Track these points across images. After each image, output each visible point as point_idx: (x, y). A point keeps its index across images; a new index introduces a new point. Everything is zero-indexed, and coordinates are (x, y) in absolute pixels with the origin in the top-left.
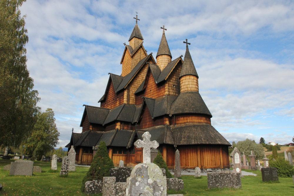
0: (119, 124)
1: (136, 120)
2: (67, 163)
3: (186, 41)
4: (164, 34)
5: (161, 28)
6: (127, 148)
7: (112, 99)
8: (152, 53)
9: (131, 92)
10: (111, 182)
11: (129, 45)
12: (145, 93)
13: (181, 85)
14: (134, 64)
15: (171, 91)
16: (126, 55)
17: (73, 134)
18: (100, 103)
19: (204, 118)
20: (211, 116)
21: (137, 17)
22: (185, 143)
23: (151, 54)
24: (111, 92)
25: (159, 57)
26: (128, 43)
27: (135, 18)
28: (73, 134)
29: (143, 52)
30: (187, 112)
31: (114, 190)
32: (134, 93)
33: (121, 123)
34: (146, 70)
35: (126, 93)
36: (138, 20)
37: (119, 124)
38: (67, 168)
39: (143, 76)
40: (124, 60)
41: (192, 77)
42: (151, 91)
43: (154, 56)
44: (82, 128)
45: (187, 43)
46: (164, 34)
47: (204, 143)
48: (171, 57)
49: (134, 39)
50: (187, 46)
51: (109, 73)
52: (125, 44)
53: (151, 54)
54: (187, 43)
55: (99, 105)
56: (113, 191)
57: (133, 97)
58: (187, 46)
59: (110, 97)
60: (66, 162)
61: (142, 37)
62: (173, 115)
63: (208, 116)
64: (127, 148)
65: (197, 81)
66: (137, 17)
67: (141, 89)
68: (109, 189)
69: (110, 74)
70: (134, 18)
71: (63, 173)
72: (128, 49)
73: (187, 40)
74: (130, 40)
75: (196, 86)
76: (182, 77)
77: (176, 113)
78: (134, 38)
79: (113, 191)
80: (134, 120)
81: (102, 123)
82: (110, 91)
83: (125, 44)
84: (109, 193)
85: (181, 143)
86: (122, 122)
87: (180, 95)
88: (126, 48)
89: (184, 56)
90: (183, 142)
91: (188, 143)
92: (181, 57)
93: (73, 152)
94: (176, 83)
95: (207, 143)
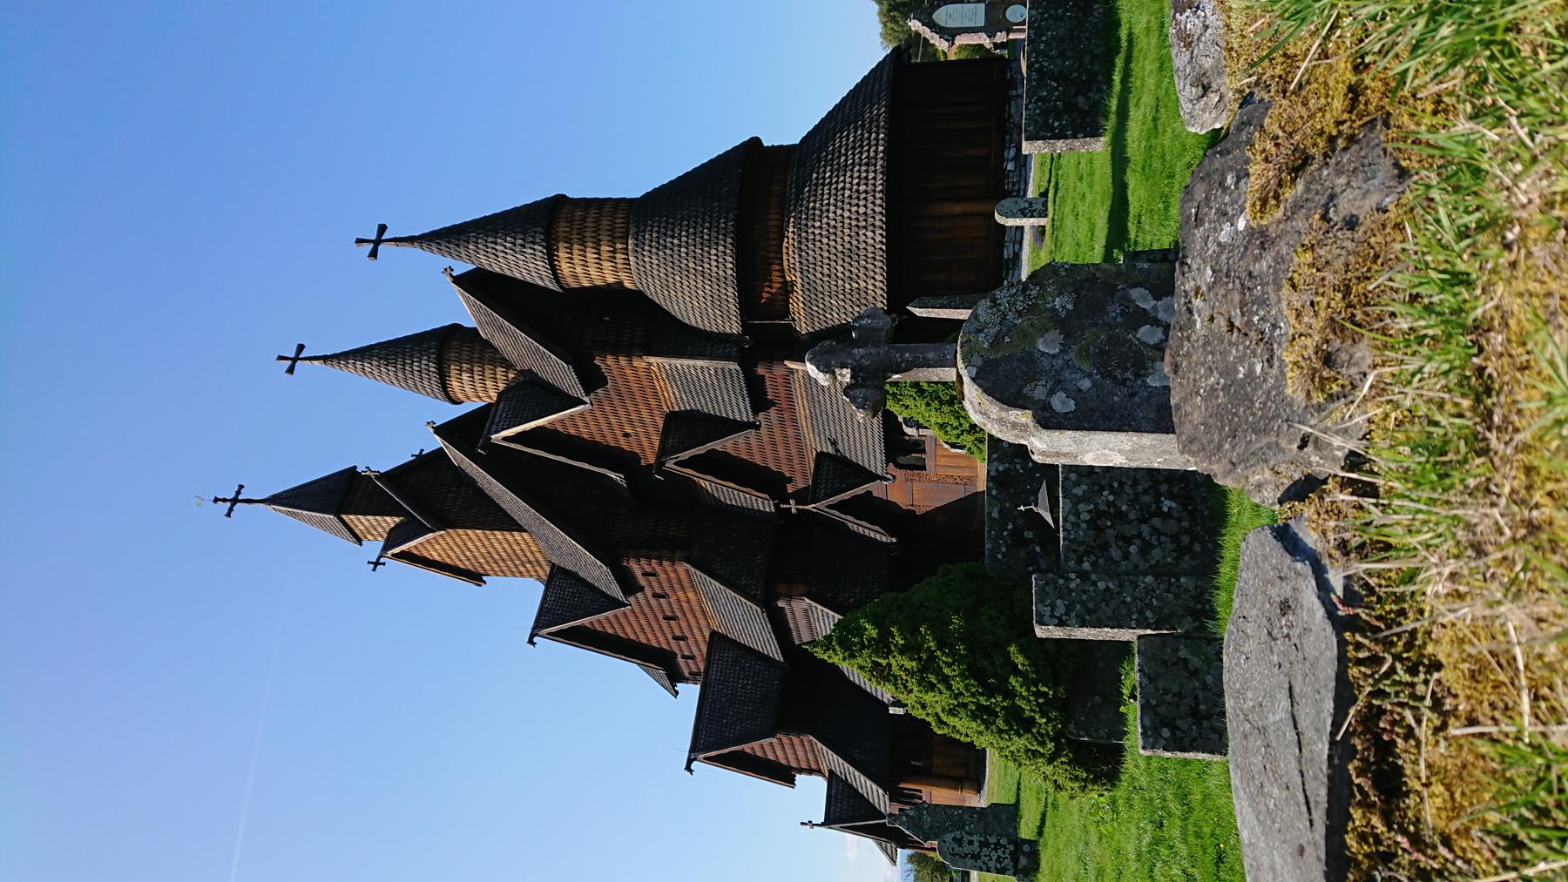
2: (971, 843)
3: (369, 247)
5: (291, 370)
7: (664, 623)
10: (1061, 598)
11: (381, 544)
13: (599, 283)
17: (829, 822)
18: (680, 687)
20: (756, 142)
21: (224, 500)
26: (373, 547)
27: (231, 510)
28: (829, 822)
31: (1094, 584)
36: (238, 493)
38: (997, 844)
42: (626, 435)
44: (800, 778)
45: (377, 242)
48: (456, 328)
51: (531, 642)
52: (377, 564)
53: (440, 430)
54: (377, 242)
56: (1101, 585)
60: (966, 849)
66: (224, 500)
68: (1091, 605)
69: (536, 639)
70: (228, 515)
71: (1020, 867)
72: (404, 547)
74: (359, 541)
75: (607, 208)
76: (556, 277)
78: (344, 517)
79: (1101, 585)
83: (377, 564)
84: (1113, 604)
85: (879, 292)
92: (459, 280)
93: (920, 818)
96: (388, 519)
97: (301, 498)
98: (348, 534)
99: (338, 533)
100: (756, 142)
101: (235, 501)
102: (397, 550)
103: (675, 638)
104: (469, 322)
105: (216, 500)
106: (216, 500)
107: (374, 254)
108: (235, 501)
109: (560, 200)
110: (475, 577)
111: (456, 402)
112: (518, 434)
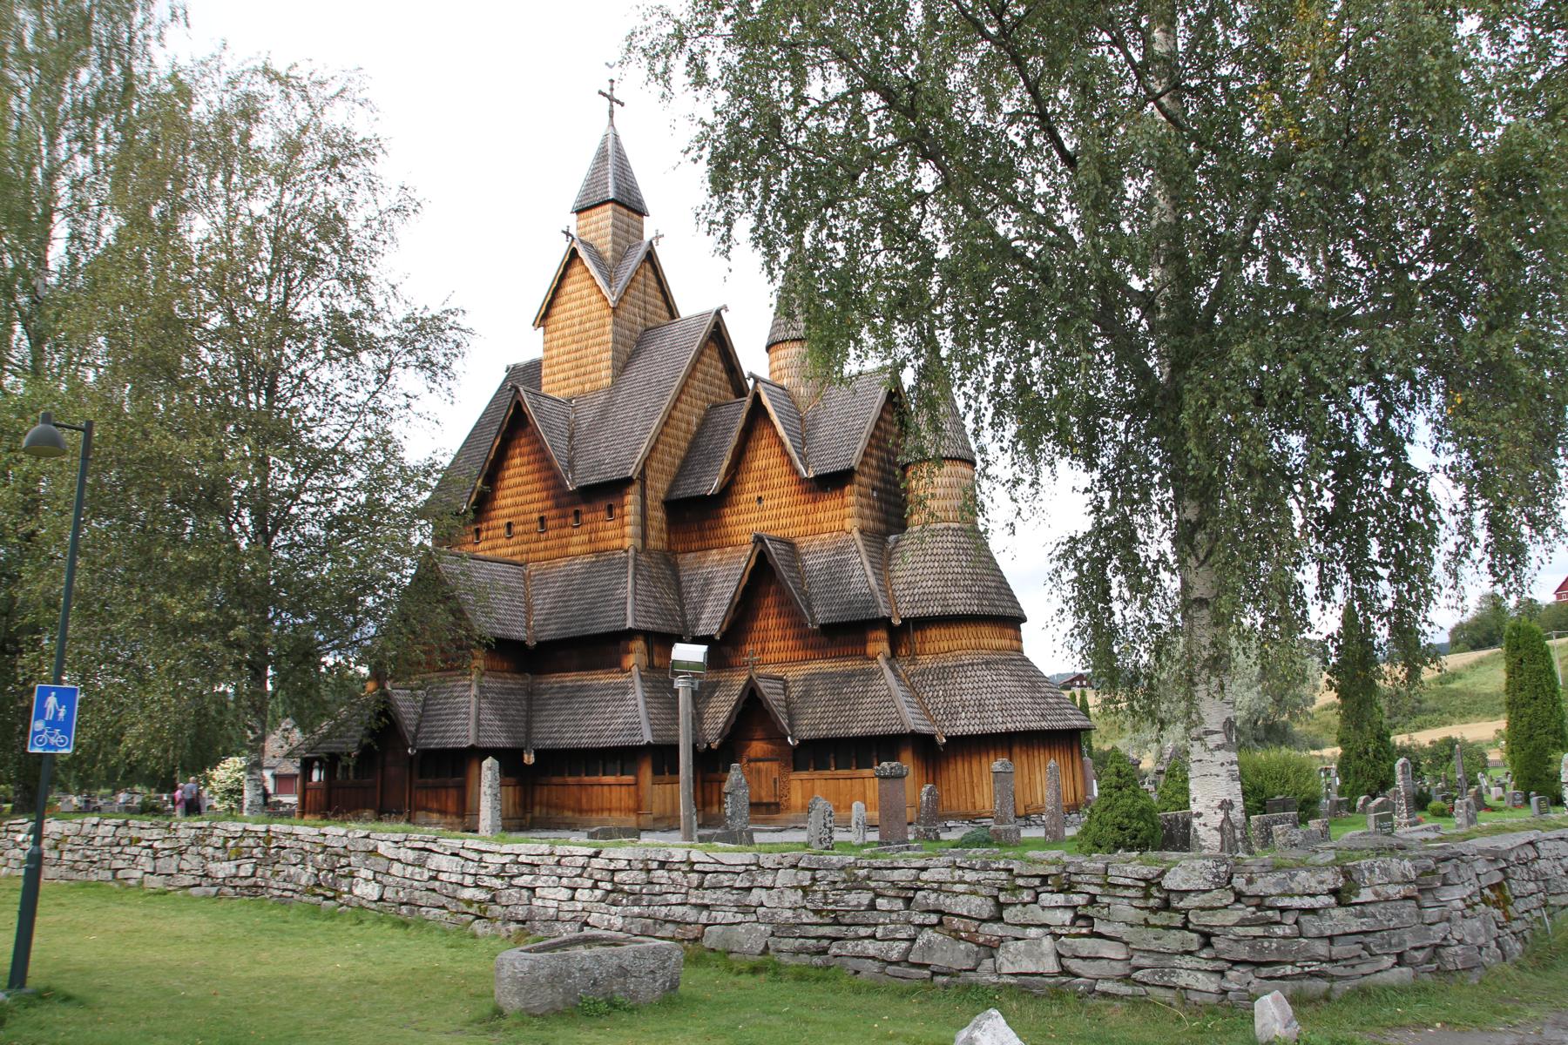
0: (638, 645)
8: (725, 308)
9: (650, 493)
12: (732, 505)
14: (624, 345)
15: (867, 512)
20: (1024, 620)
22: (975, 728)
29: (654, 284)
30: (960, 609)
32: (662, 496)
35: (631, 500)
40: (555, 311)
42: (760, 499)
47: (1034, 725)
49: (610, 213)
52: (568, 234)
57: (657, 515)
59: (509, 501)
61: (640, 202)
62: (905, 621)
67: (713, 485)
70: (601, 93)
74: (578, 212)
77: (919, 612)
78: (609, 206)
80: (697, 626)
82: (507, 474)
83: (568, 234)
88: (573, 254)
90: (966, 725)
91: (988, 729)
94: (882, 480)
95: (1045, 725)
96: (610, 246)
98: (586, 203)
99: (585, 193)
100: (1024, 620)
101: (611, 99)
102: (582, 253)
103: (509, 525)
105: (612, 81)
106: (612, 81)
108: (611, 99)
110: (544, 318)
112: (764, 408)
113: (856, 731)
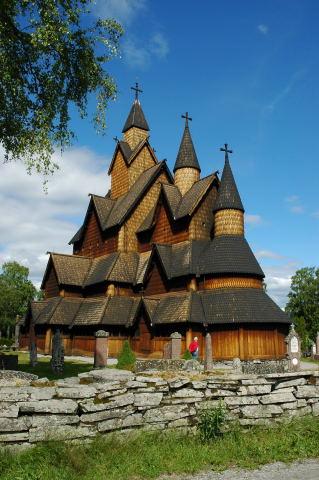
0: (112, 286)
1: (140, 281)
4: (187, 127)
6: (127, 326)
16: (117, 162)
18: (72, 245)
19: (252, 280)
23: (164, 162)
24: (92, 227)
25: (179, 171)
26: (122, 137)
33: (116, 286)
34: (155, 190)
35: (121, 233)
37: (112, 286)
39: (151, 201)
41: (234, 212)
43: (171, 166)
46: (187, 127)
48: (199, 171)
50: (227, 157)
53: (164, 162)
54: (226, 150)
55: (69, 250)
58: (227, 157)
62: (202, 276)
63: (260, 277)
64: (127, 326)
65: (242, 217)
73: (226, 145)
77: (207, 271)
81: (81, 284)
86: (118, 284)
87: (215, 240)
89: (221, 171)
92: (215, 174)
97: (136, 109)
104: (203, 175)
107: (222, 150)
109: (243, 211)
111: (174, 171)
113: (173, 320)
